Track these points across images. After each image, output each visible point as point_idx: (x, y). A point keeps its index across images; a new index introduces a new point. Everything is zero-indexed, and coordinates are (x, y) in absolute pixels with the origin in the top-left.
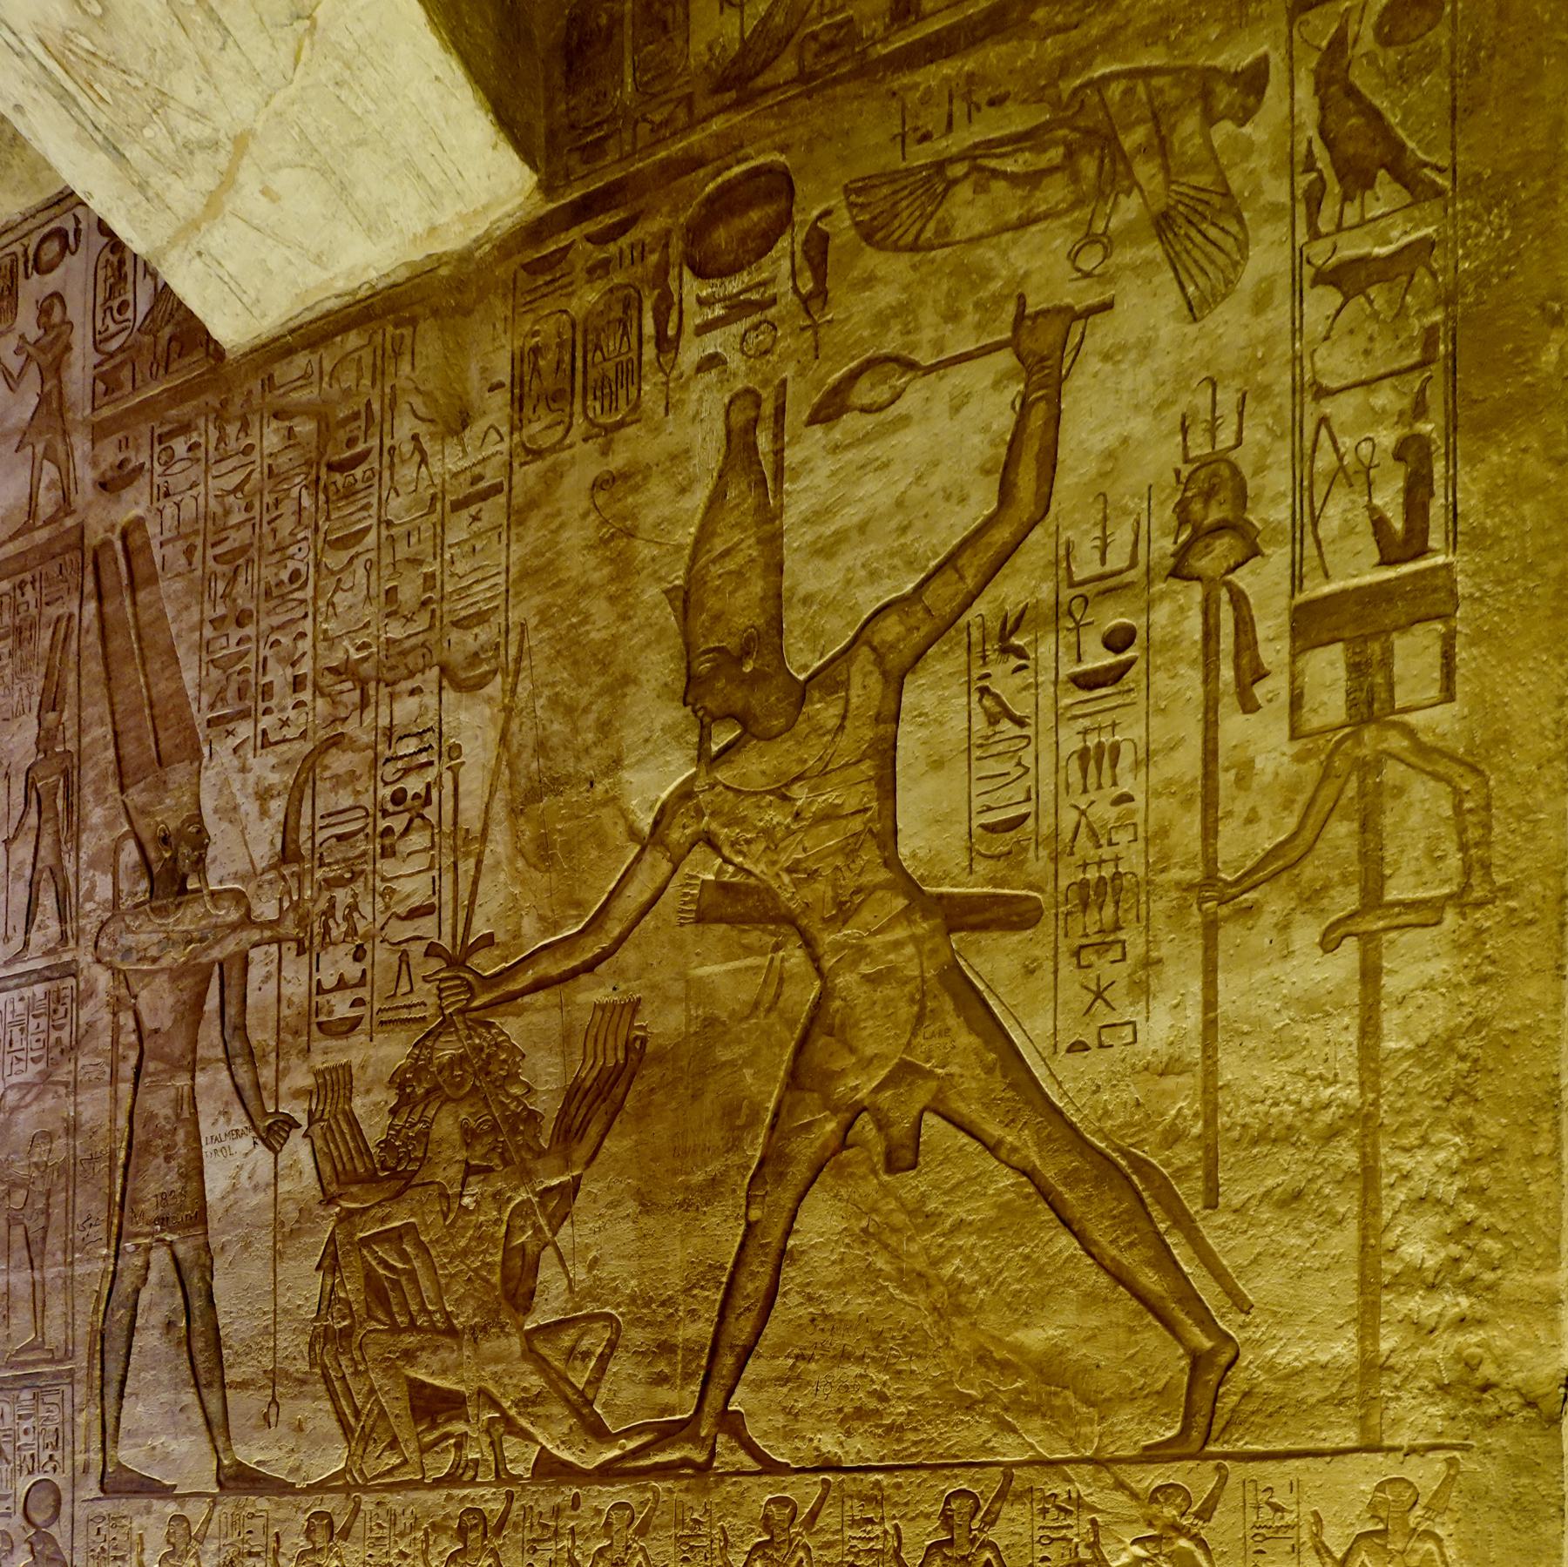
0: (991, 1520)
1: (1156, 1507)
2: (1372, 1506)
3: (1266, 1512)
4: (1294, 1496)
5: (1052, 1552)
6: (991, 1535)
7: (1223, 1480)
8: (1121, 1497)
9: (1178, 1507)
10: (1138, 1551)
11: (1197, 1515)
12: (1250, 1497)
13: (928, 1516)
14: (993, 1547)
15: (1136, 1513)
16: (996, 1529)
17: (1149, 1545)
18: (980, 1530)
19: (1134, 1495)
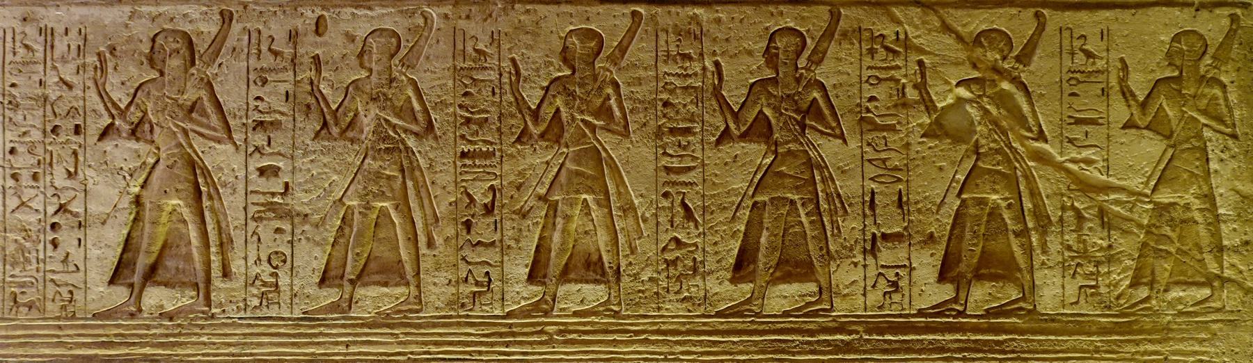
0: (818, 58)
1: (979, 51)
2: (1169, 55)
3: (1080, 58)
4: (1103, 45)
5: (881, 92)
6: (821, 73)
7: (1041, 27)
8: (949, 40)
9: (1002, 51)
10: (963, 92)
11: (1018, 59)
12: (1066, 43)
13: (750, 53)
14: (822, 87)
15: (962, 55)
16: (824, 67)
17: (974, 87)
18: (808, 69)
19: (960, 38)
